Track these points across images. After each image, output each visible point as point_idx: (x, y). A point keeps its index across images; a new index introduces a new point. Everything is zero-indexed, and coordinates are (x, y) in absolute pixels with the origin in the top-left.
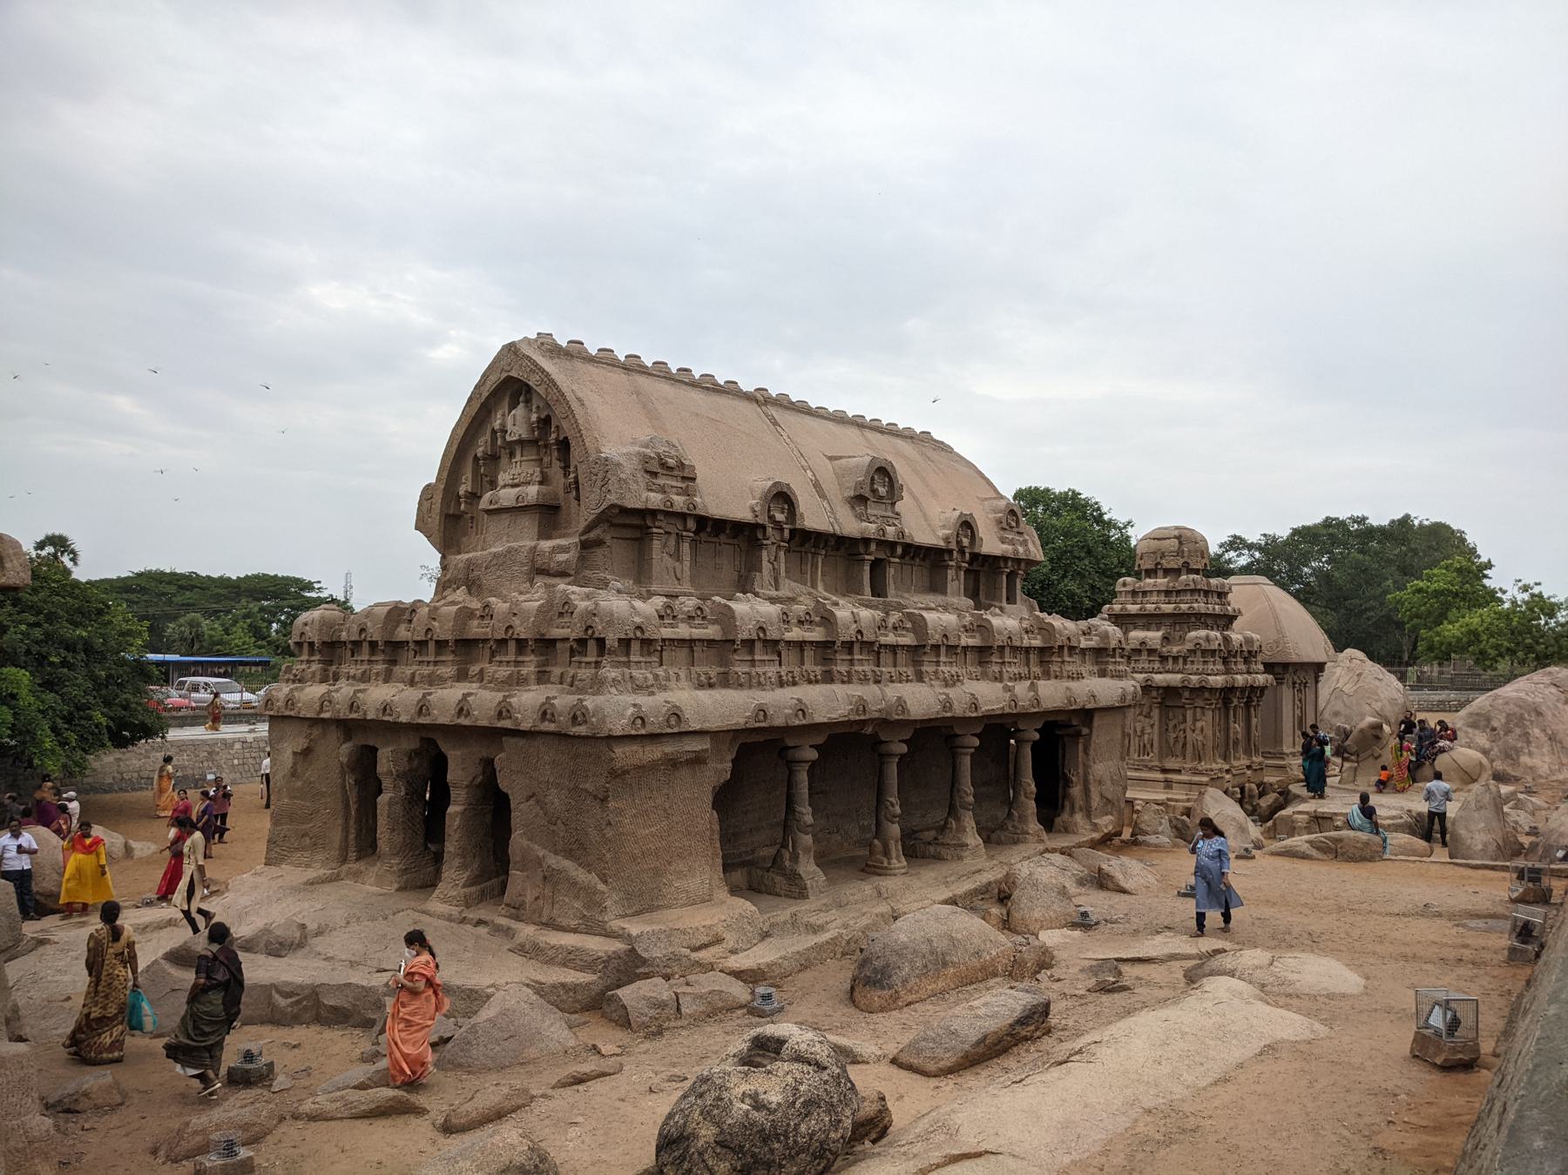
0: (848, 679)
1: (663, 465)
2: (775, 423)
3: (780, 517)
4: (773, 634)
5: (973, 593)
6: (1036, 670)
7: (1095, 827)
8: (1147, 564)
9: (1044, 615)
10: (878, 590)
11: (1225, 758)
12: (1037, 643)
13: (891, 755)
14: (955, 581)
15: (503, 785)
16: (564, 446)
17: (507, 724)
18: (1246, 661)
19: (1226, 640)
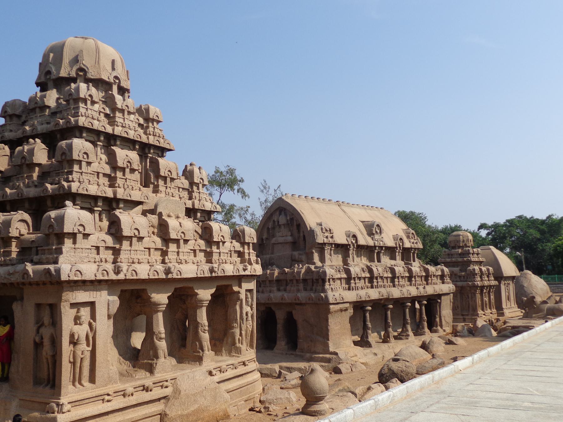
0: (377, 287)
1: (326, 230)
2: (345, 212)
3: (354, 242)
4: (360, 276)
5: (402, 260)
6: (425, 282)
7: (444, 331)
8: (452, 245)
9: (425, 266)
10: (379, 261)
11: (483, 310)
12: (424, 274)
13: (389, 308)
14: (398, 257)
15: (295, 317)
16: (298, 226)
17: (297, 302)
18: (488, 277)
19: (481, 270)
